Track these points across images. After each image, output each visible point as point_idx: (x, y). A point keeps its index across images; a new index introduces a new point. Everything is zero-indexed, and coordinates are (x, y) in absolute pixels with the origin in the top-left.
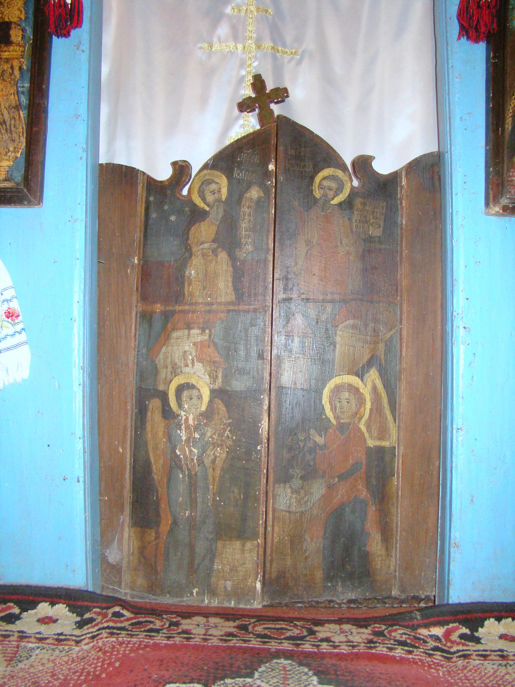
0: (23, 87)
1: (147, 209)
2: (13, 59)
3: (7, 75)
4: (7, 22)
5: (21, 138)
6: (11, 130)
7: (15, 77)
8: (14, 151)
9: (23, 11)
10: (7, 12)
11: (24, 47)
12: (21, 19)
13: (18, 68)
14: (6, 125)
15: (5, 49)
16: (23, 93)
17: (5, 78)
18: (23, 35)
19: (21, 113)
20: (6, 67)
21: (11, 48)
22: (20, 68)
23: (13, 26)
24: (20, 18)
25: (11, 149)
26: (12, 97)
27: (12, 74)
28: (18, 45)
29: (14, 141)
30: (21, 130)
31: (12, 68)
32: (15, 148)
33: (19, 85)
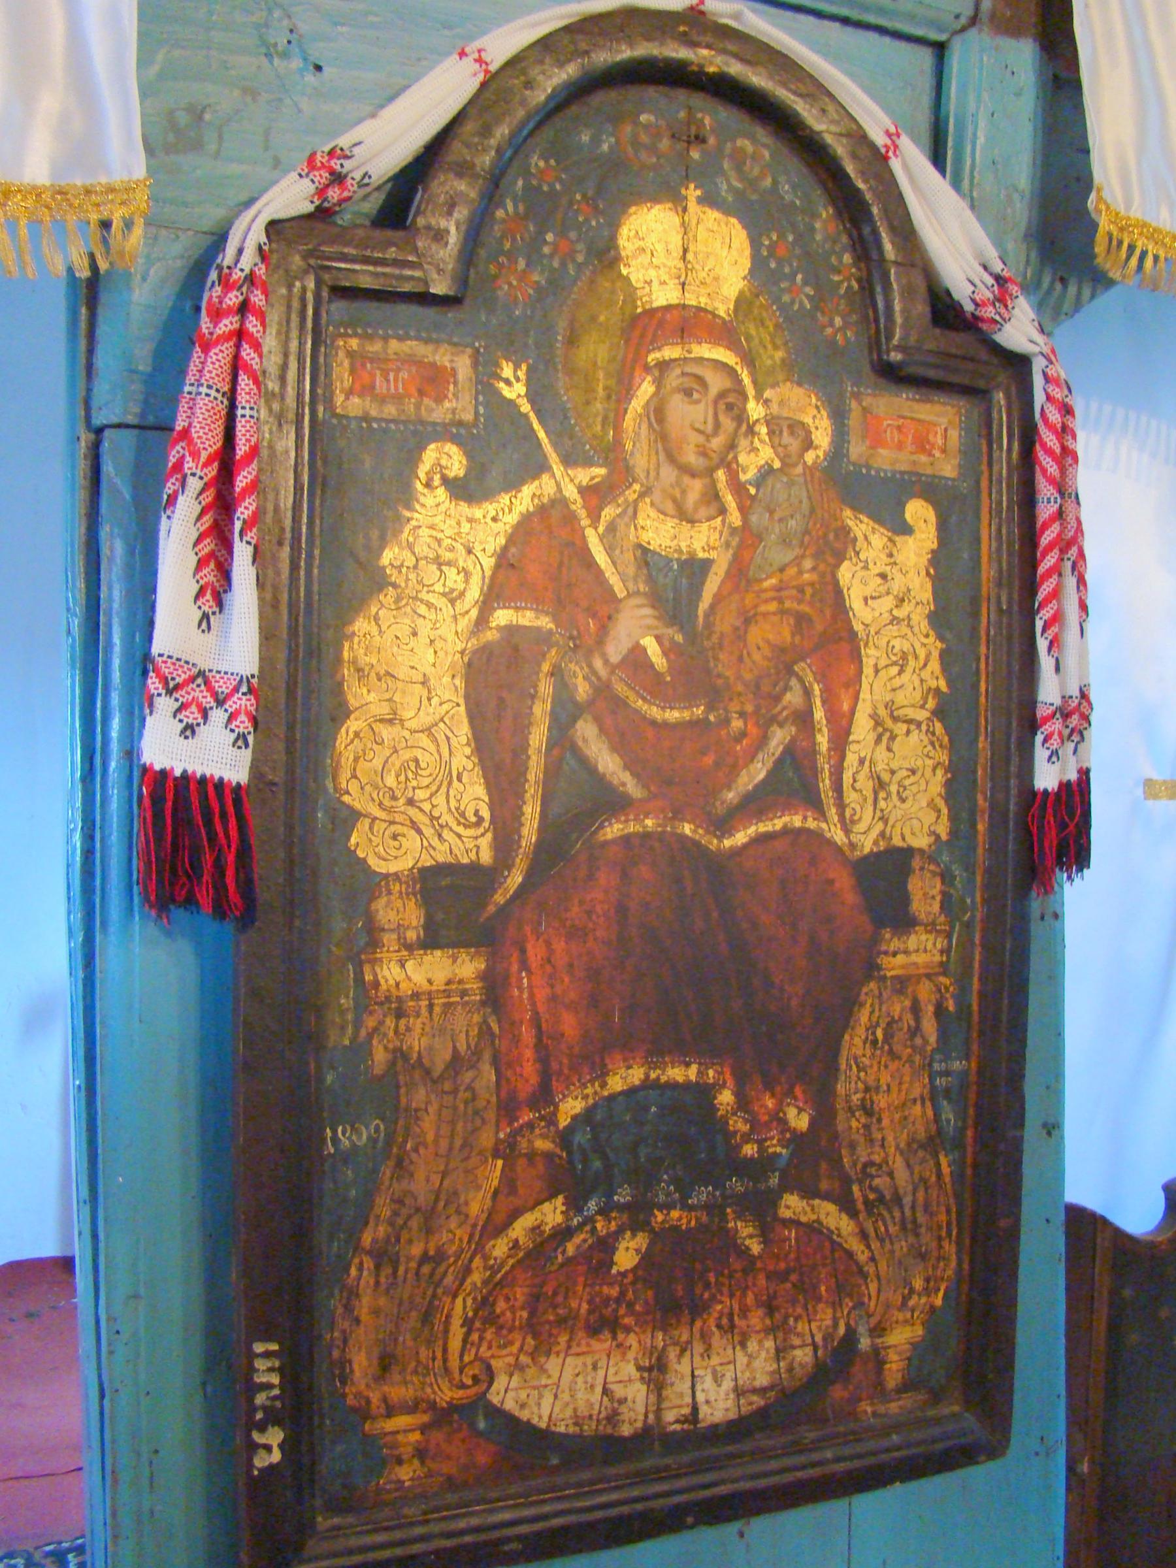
0: (947, 1073)
1: (1114, 1328)
2: (918, 978)
3: (900, 1036)
4: (900, 850)
5: (946, 1244)
6: (914, 1221)
7: (926, 1042)
8: (927, 1291)
9: (945, 811)
10: (899, 813)
11: (949, 936)
12: (938, 837)
13: (931, 1008)
14: (901, 1207)
15: (895, 944)
16: (947, 1092)
17: (897, 1048)
18: (943, 893)
19: (944, 1161)
20: (898, 1007)
21: (912, 942)
22: (940, 1011)
23: (916, 863)
24: (934, 833)
25: (918, 1284)
26: (917, 1109)
27: (916, 1031)
28: (931, 927)
29: (923, 1257)
30: (943, 1217)
31: (916, 1009)
32: (927, 1280)
33: (936, 1066)
